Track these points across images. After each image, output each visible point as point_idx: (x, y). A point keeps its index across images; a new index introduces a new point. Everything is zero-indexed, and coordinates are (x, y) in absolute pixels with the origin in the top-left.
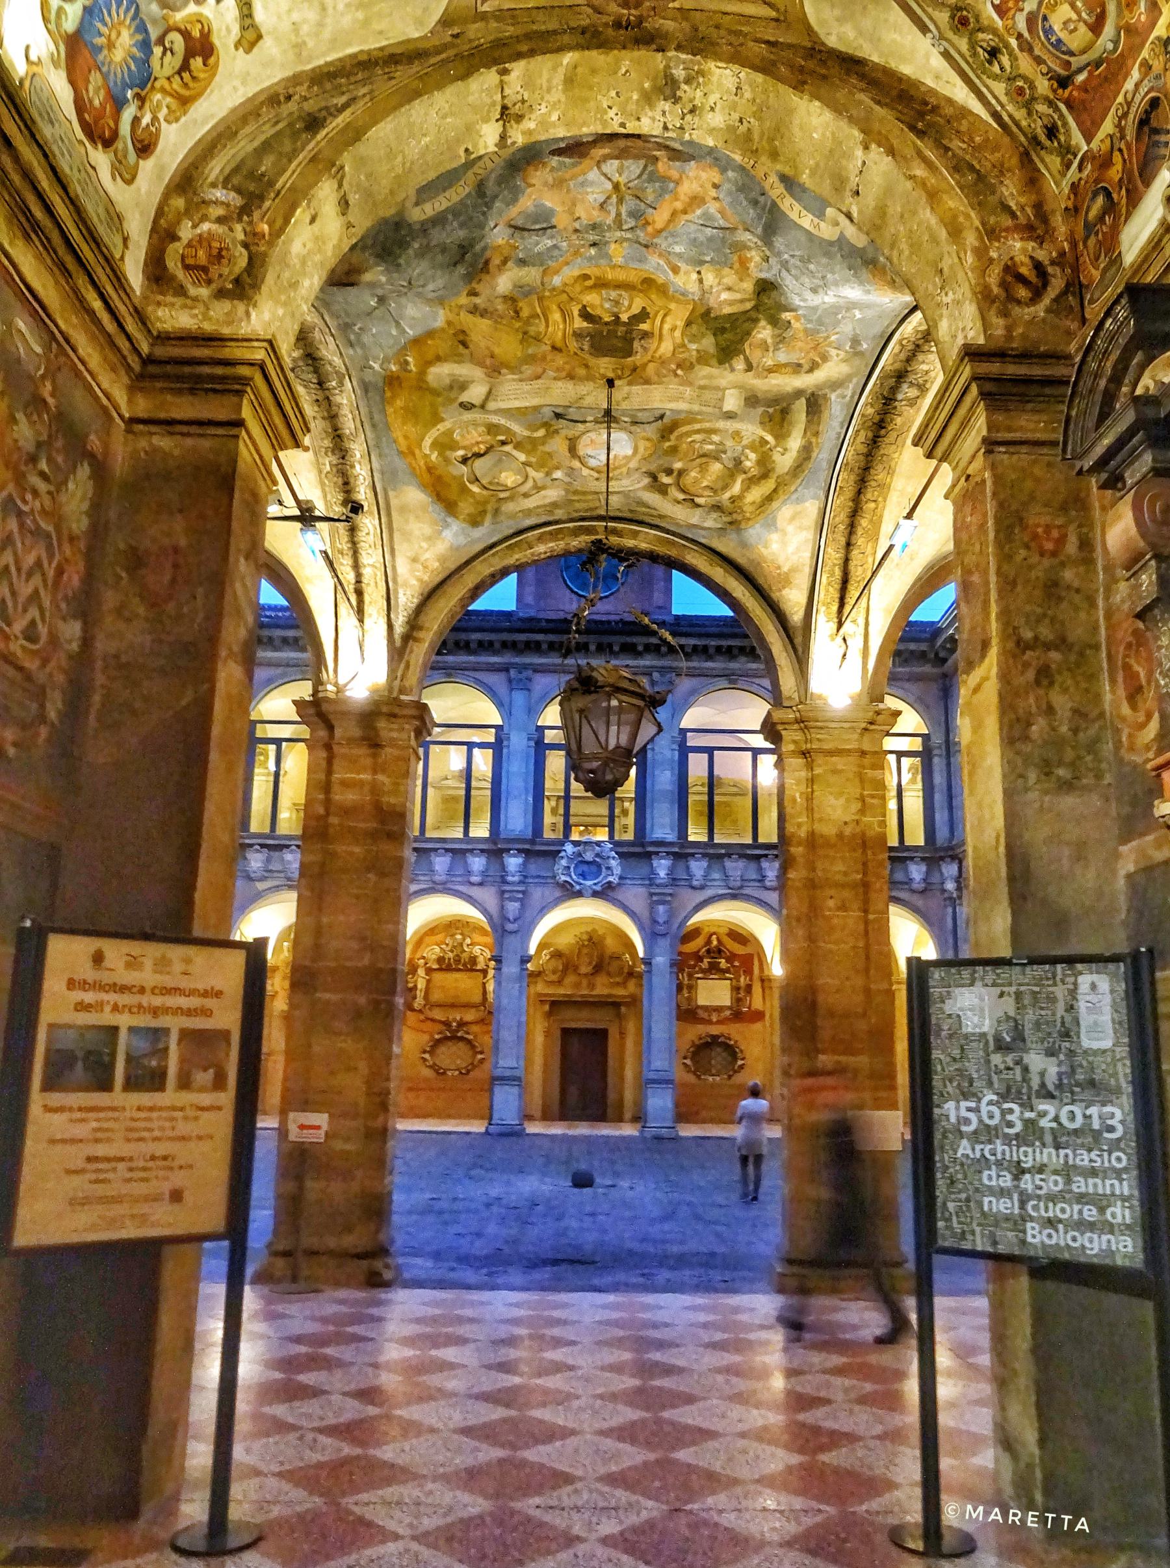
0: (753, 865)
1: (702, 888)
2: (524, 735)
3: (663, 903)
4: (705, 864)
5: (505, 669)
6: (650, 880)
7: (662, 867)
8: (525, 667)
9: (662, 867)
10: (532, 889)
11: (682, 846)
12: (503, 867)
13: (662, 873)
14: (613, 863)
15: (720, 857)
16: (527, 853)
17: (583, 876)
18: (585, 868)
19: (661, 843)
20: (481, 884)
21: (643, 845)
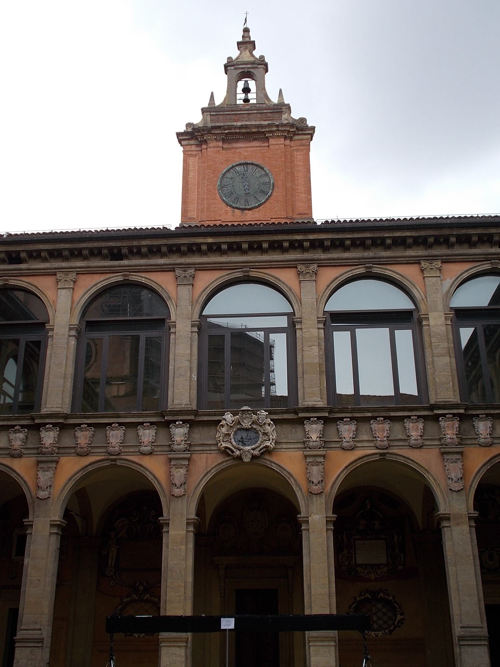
0: (398, 426)
1: (352, 449)
2: (189, 323)
3: (318, 464)
4: (353, 427)
5: (171, 268)
6: (305, 444)
7: (314, 431)
8: (188, 266)
9: (314, 431)
10: (195, 457)
11: (331, 411)
12: (170, 437)
13: (314, 437)
14: (268, 429)
15: (367, 420)
16: (192, 424)
17: (242, 442)
18: (244, 434)
19: (314, 409)
20: (151, 454)
21: (296, 412)
